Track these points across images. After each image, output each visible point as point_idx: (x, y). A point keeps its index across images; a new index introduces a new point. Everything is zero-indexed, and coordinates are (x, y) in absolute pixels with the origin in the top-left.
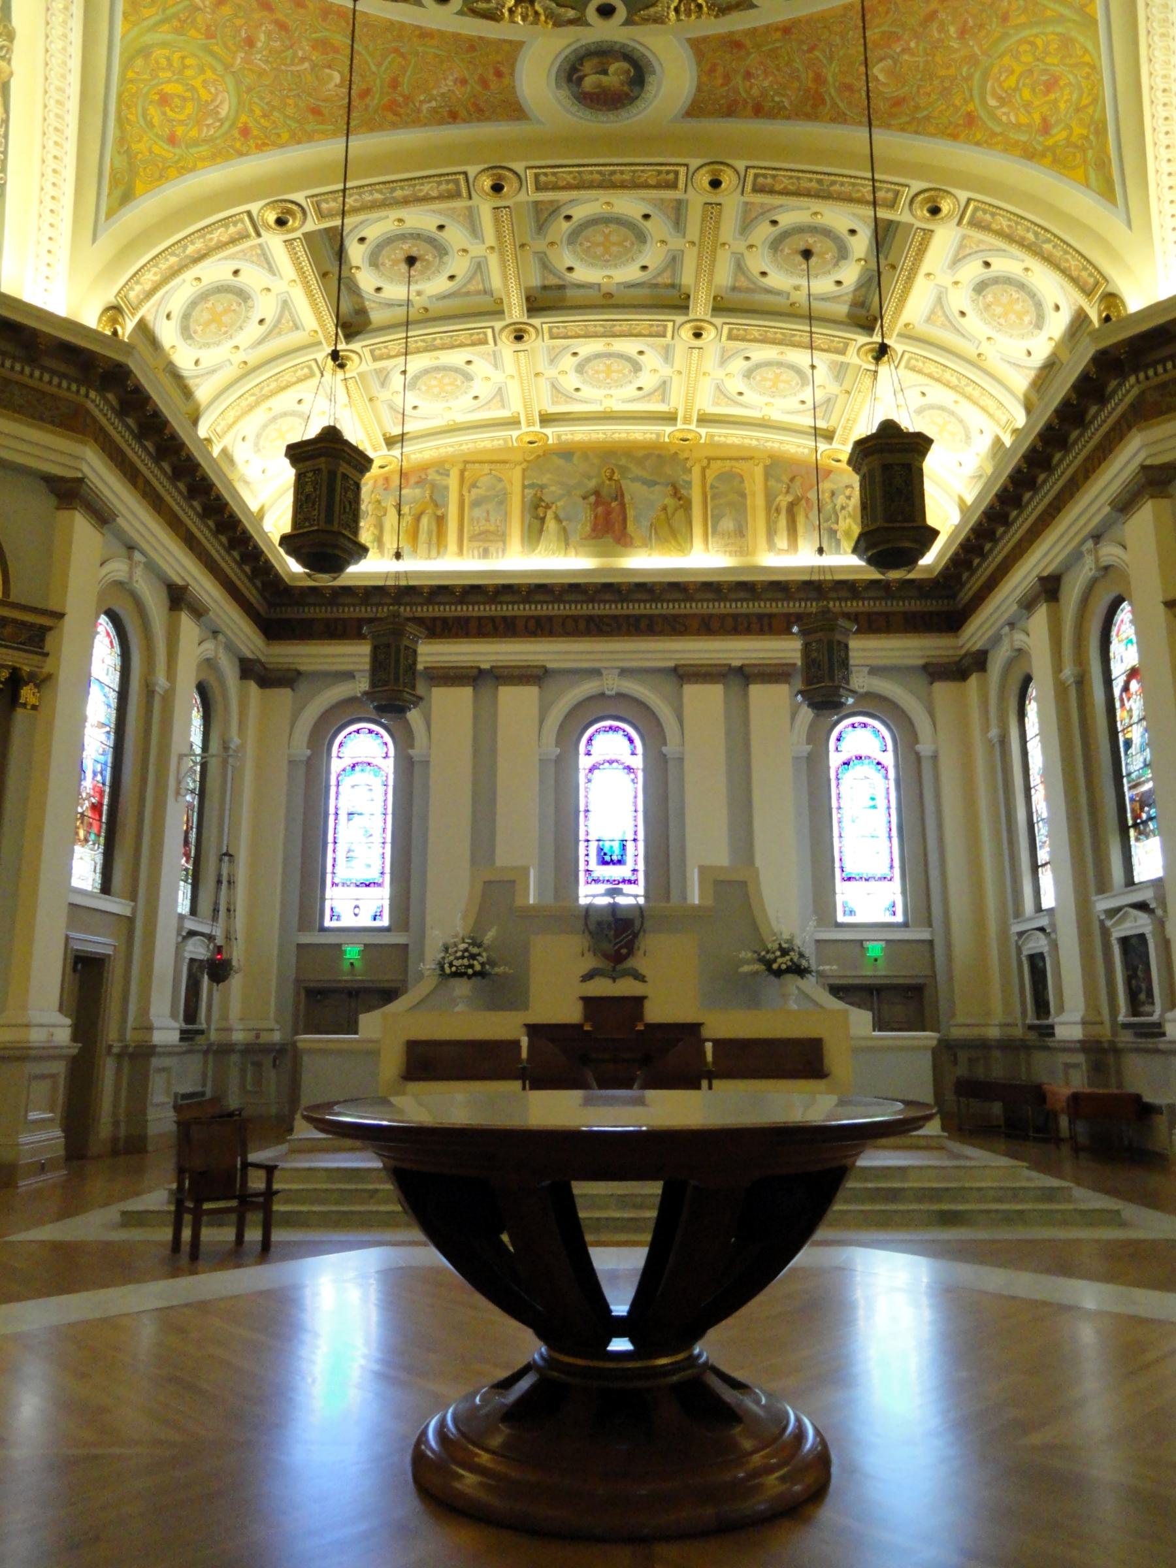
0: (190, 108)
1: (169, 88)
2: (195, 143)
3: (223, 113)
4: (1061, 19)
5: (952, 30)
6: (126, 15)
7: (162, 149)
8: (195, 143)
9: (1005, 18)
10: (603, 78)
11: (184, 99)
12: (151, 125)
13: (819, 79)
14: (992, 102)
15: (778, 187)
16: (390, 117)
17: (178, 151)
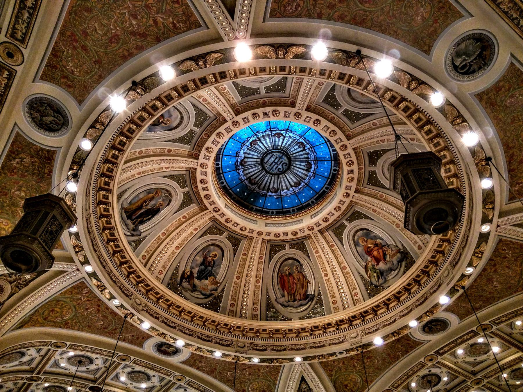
0: (58, 314)
1: (56, 309)
2: (51, 321)
3: (65, 318)
4: (270, 381)
5: (248, 373)
6: (61, 294)
7: (41, 320)
8: (51, 321)
9: (259, 376)
10: (167, 349)
11: (58, 312)
12: (43, 314)
13: (215, 369)
14: (250, 389)
15: (194, 386)
16: (108, 334)
17: (45, 322)
